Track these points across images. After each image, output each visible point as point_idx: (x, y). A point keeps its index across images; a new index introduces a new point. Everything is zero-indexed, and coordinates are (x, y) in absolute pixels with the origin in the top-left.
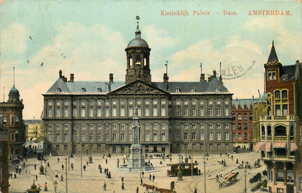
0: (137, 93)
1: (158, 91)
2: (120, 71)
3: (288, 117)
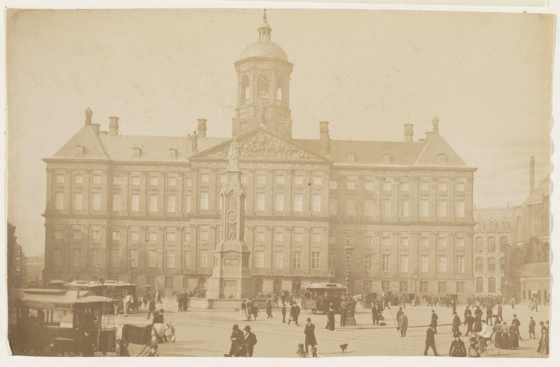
1: (306, 155)
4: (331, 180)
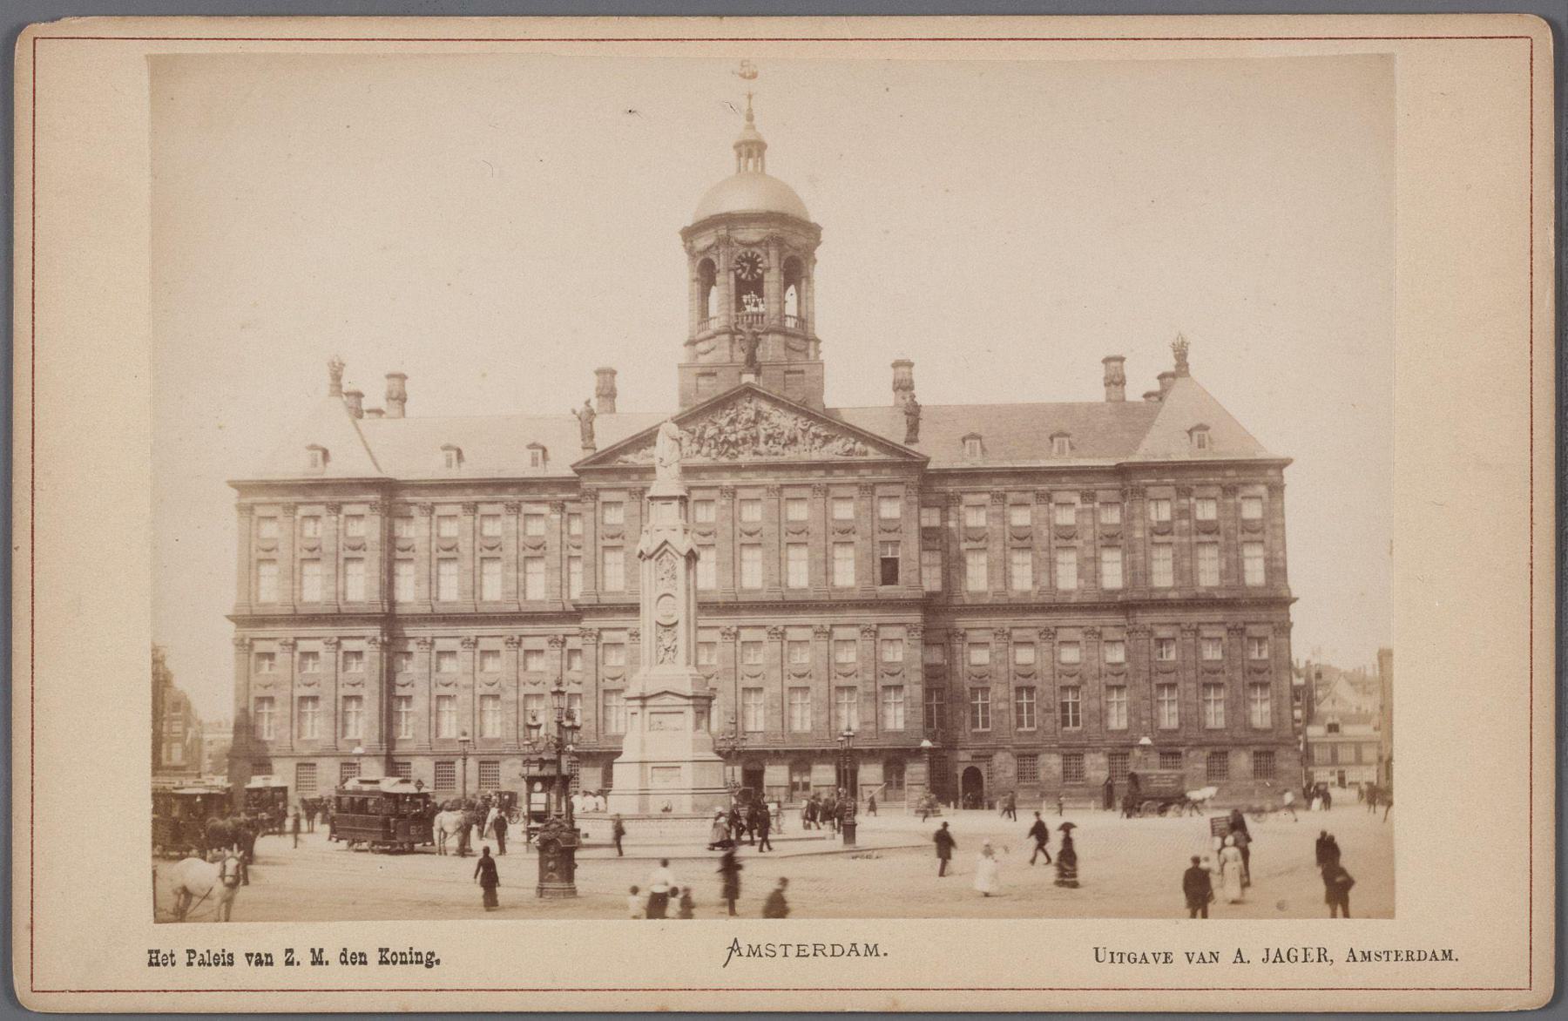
0: (745, 458)
2: (652, 347)
4: (924, 505)
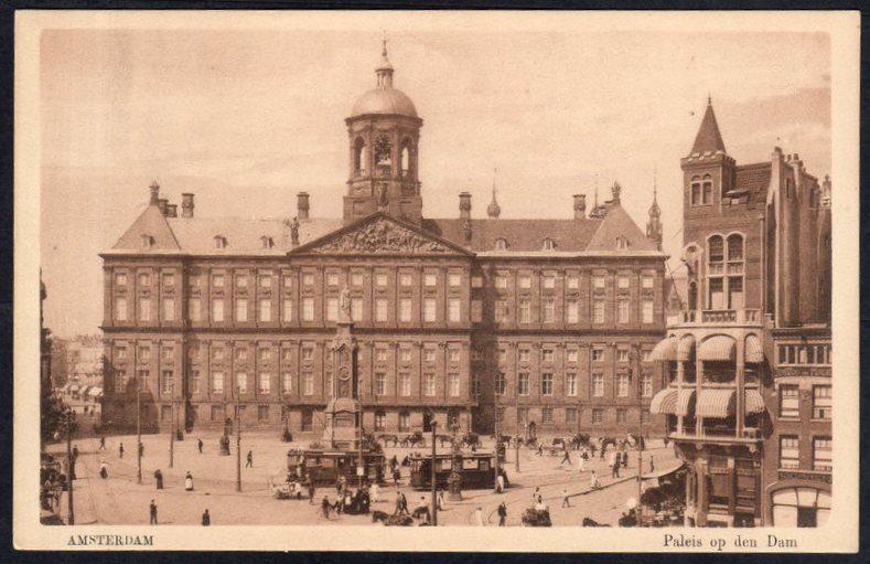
0: (378, 252)
3: (740, 315)
